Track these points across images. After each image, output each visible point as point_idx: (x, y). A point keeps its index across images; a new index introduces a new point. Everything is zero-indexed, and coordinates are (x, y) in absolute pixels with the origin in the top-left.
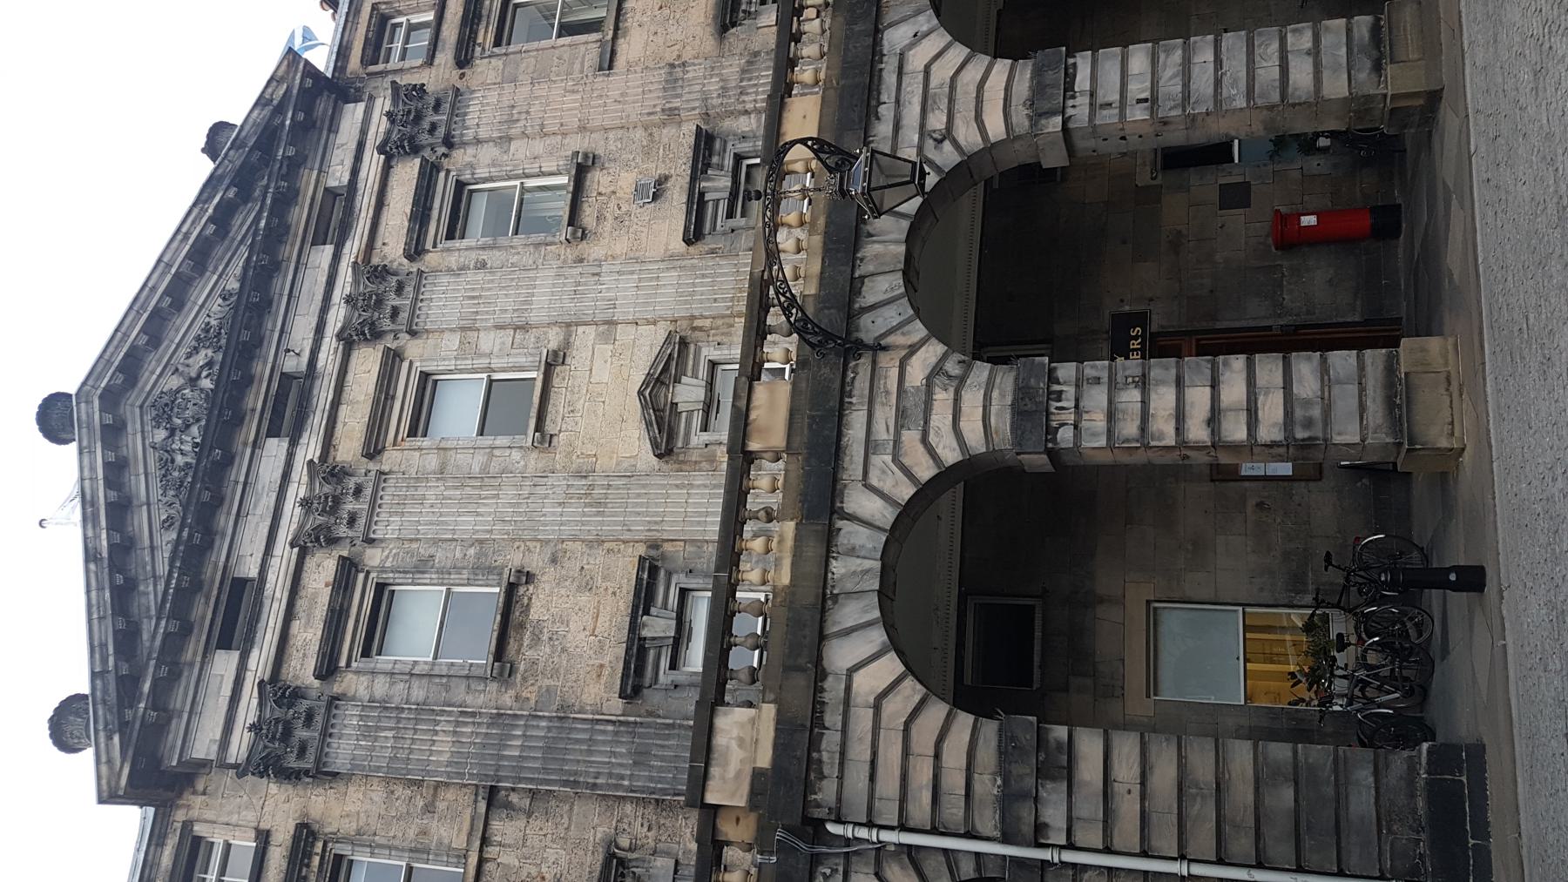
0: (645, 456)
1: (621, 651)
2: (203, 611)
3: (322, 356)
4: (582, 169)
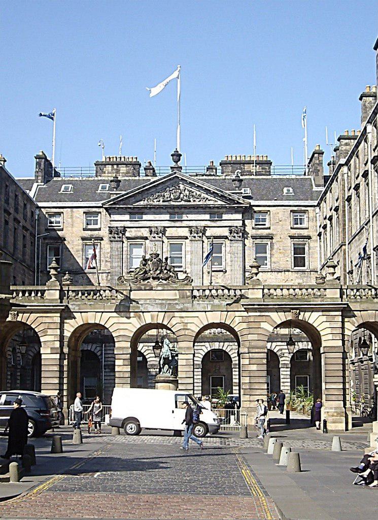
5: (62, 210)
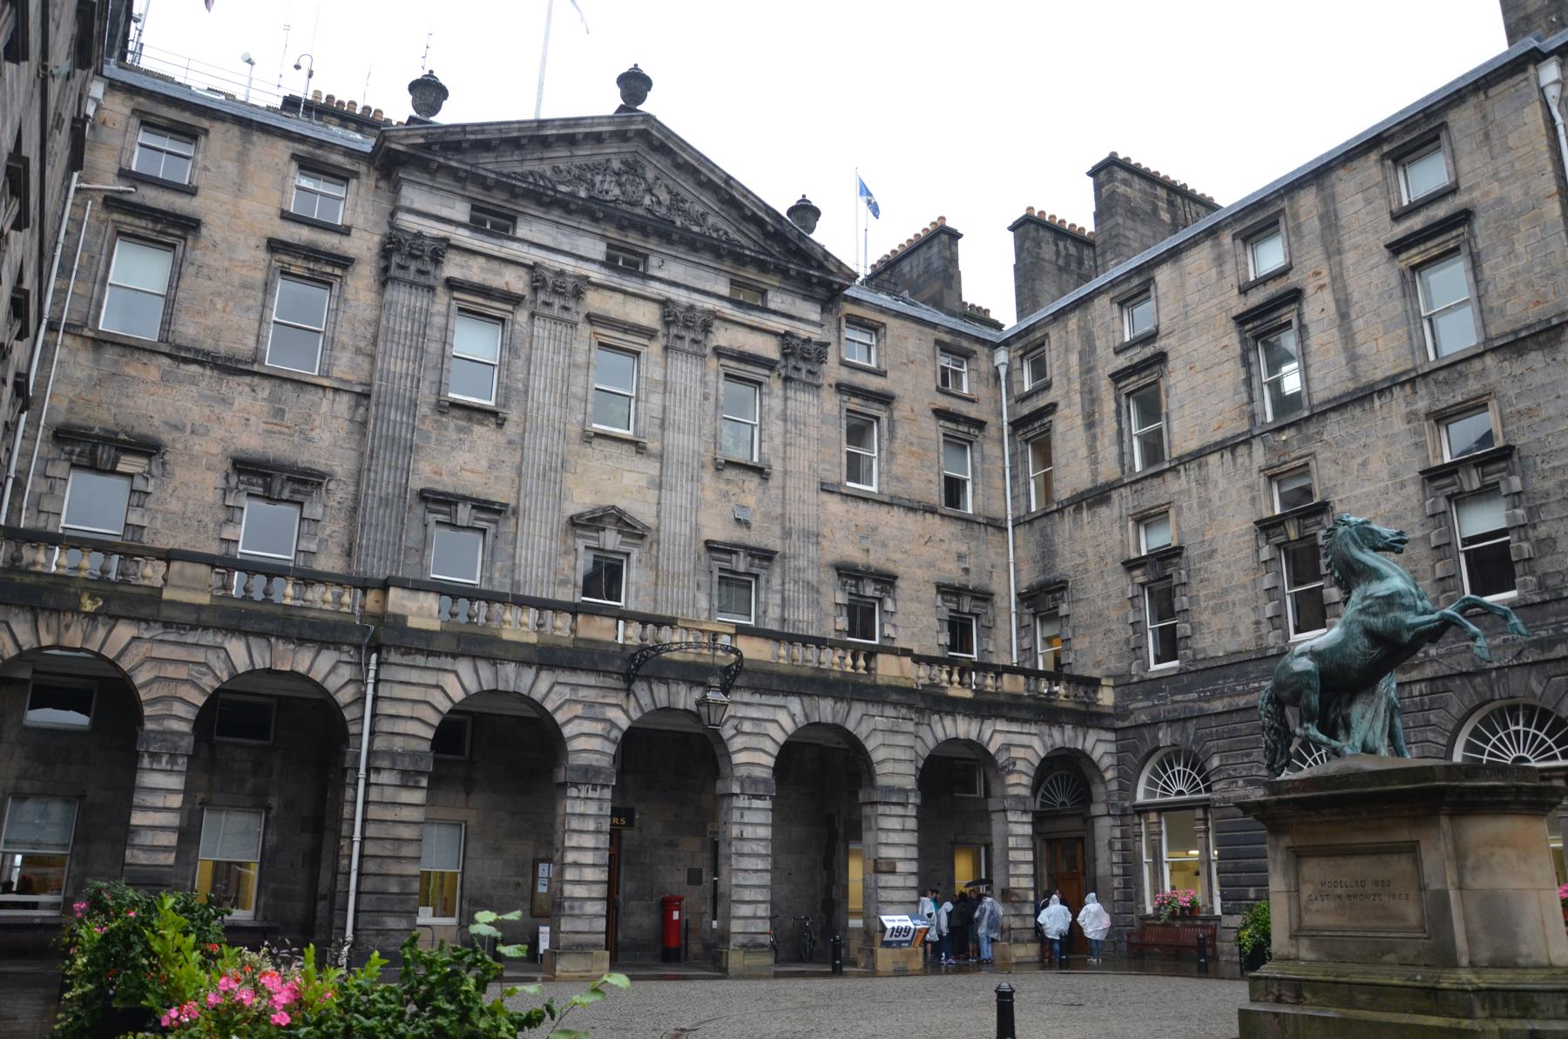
0: (572, 509)
1: (450, 489)
2: (498, 199)
3: (657, 285)
4: (761, 472)
5: (205, 123)
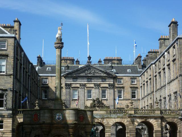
5: (48, 77)
